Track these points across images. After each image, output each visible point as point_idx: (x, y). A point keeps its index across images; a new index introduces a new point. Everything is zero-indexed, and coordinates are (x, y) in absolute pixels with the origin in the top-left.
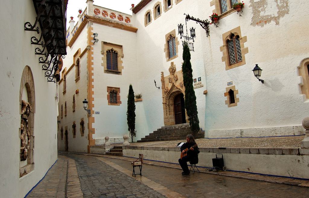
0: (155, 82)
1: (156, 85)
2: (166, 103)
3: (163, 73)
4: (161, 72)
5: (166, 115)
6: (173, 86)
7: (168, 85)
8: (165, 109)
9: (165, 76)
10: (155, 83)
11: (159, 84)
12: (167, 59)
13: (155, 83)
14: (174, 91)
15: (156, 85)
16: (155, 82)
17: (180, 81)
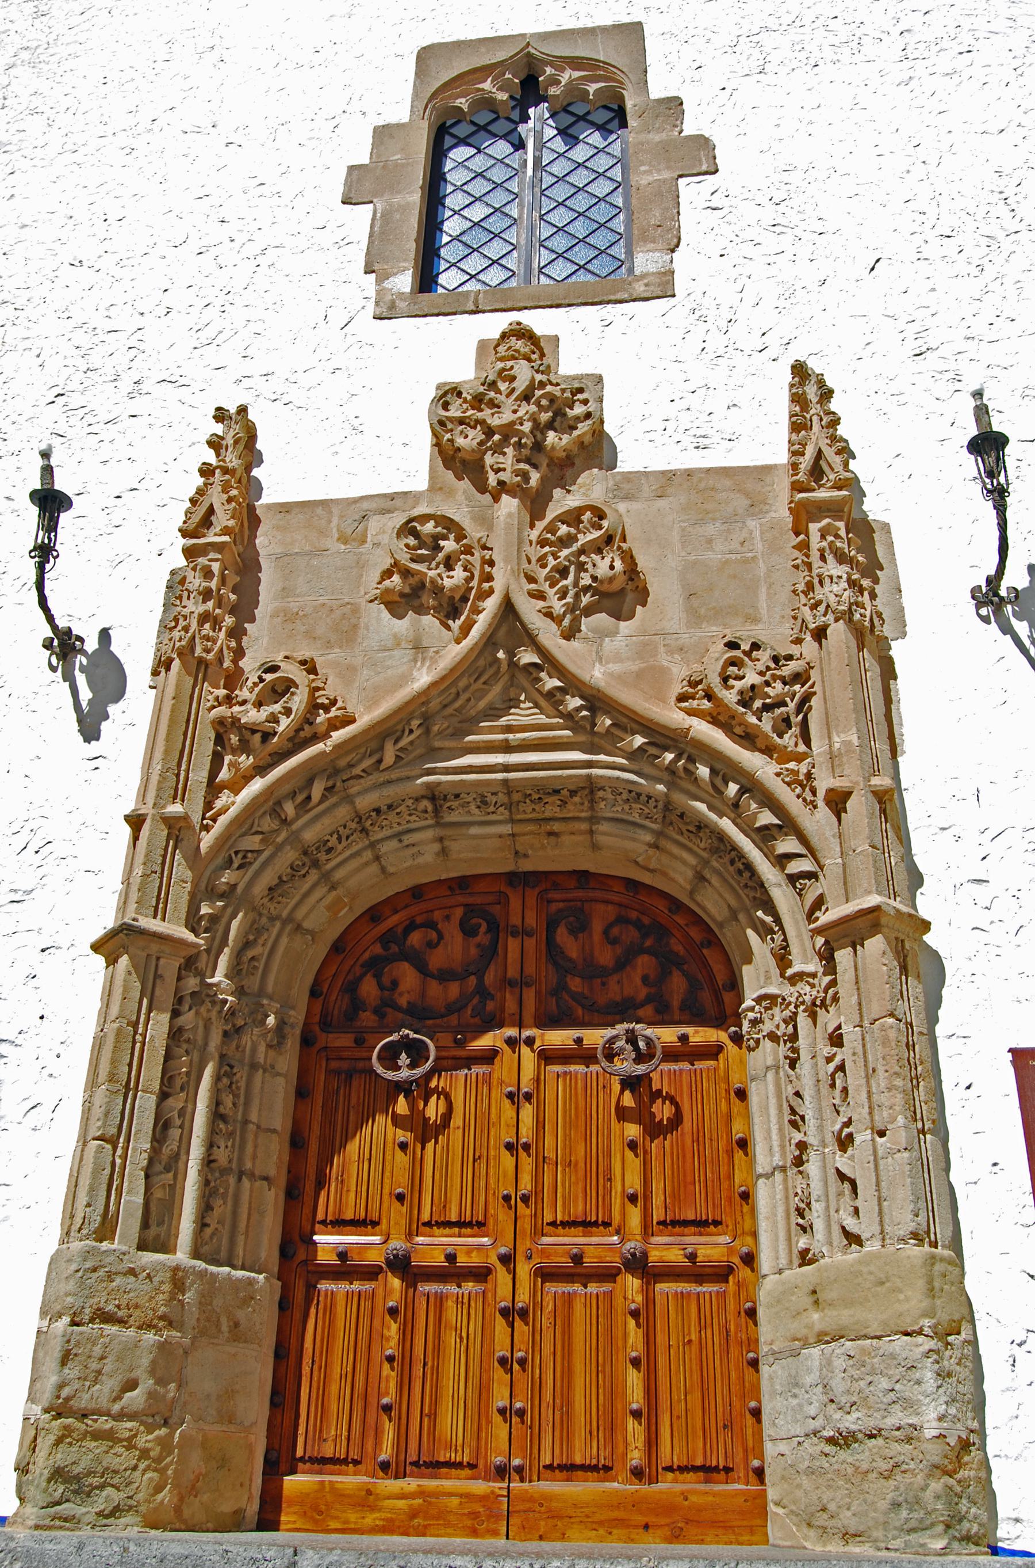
0: (50, 502)
1: (44, 553)
2: (192, 963)
3: (237, 441)
4: (220, 415)
5: (142, 1246)
6: (504, 667)
7: (348, 631)
8: (152, 1074)
9: (278, 482)
10: (49, 524)
11: (124, 583)
12: (404, 282)
13: (49, 524)
14: (474, 763)
15: (44, 553)
16: (50, 502)
17: (695, 617)
